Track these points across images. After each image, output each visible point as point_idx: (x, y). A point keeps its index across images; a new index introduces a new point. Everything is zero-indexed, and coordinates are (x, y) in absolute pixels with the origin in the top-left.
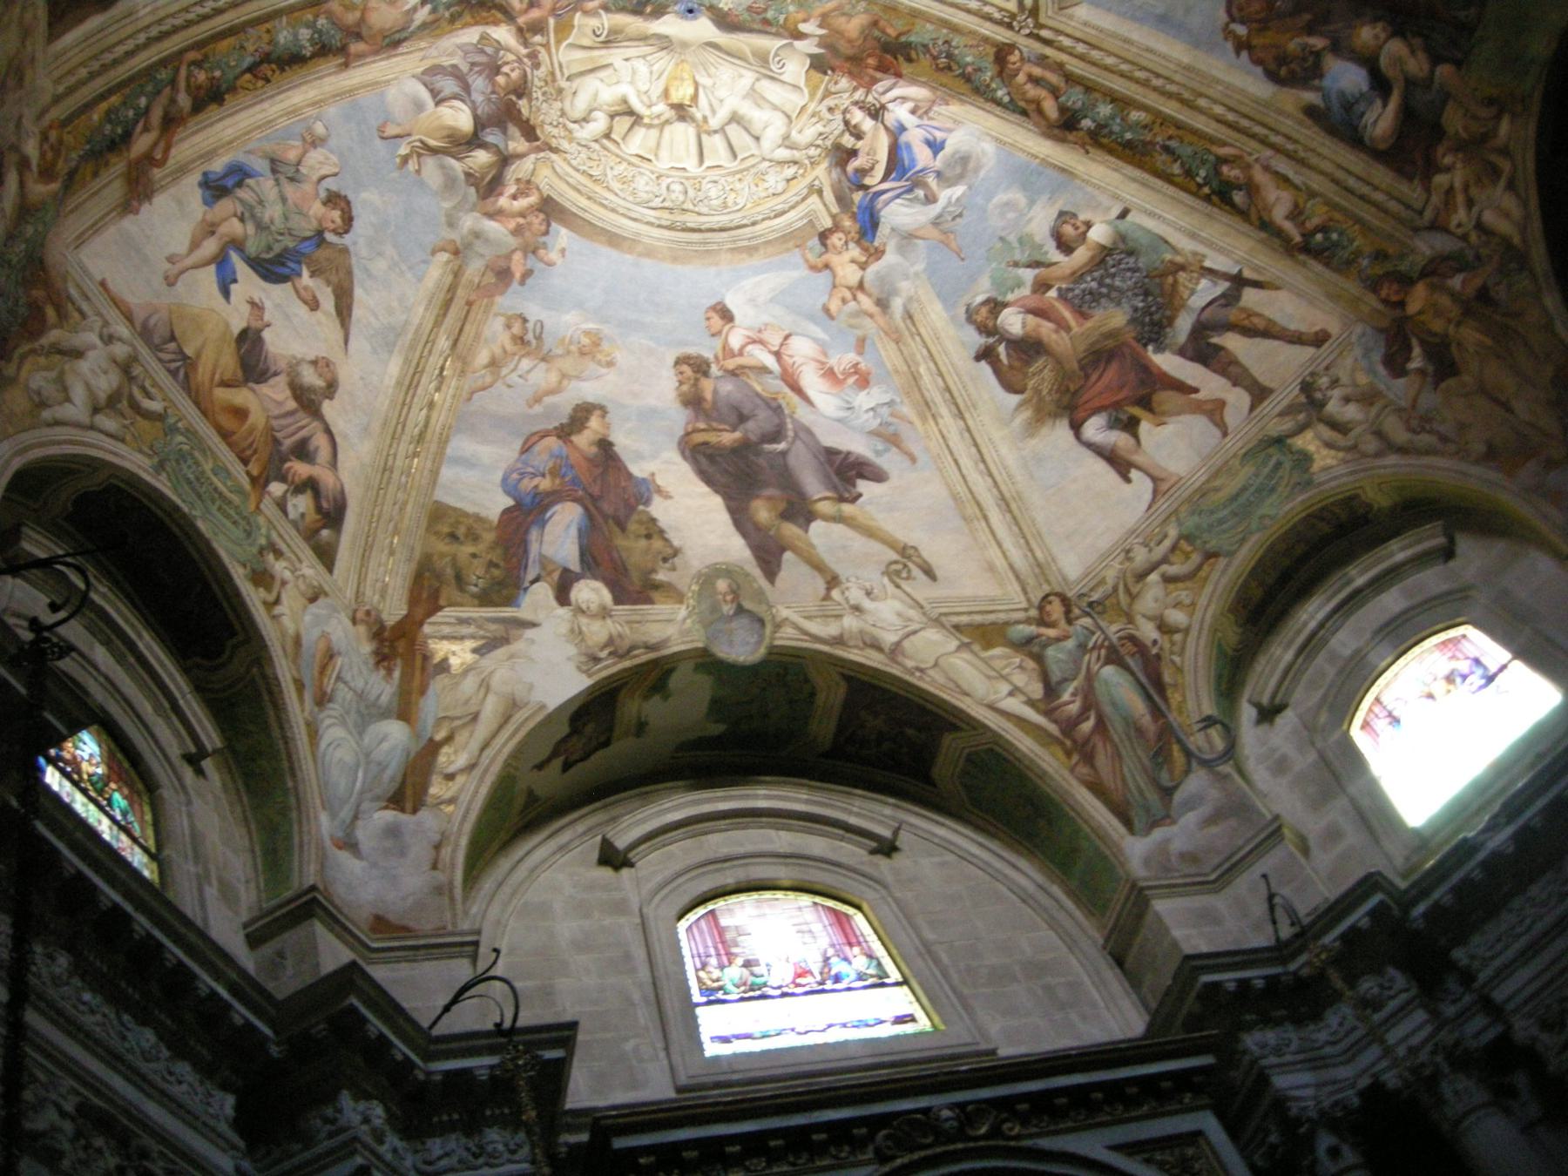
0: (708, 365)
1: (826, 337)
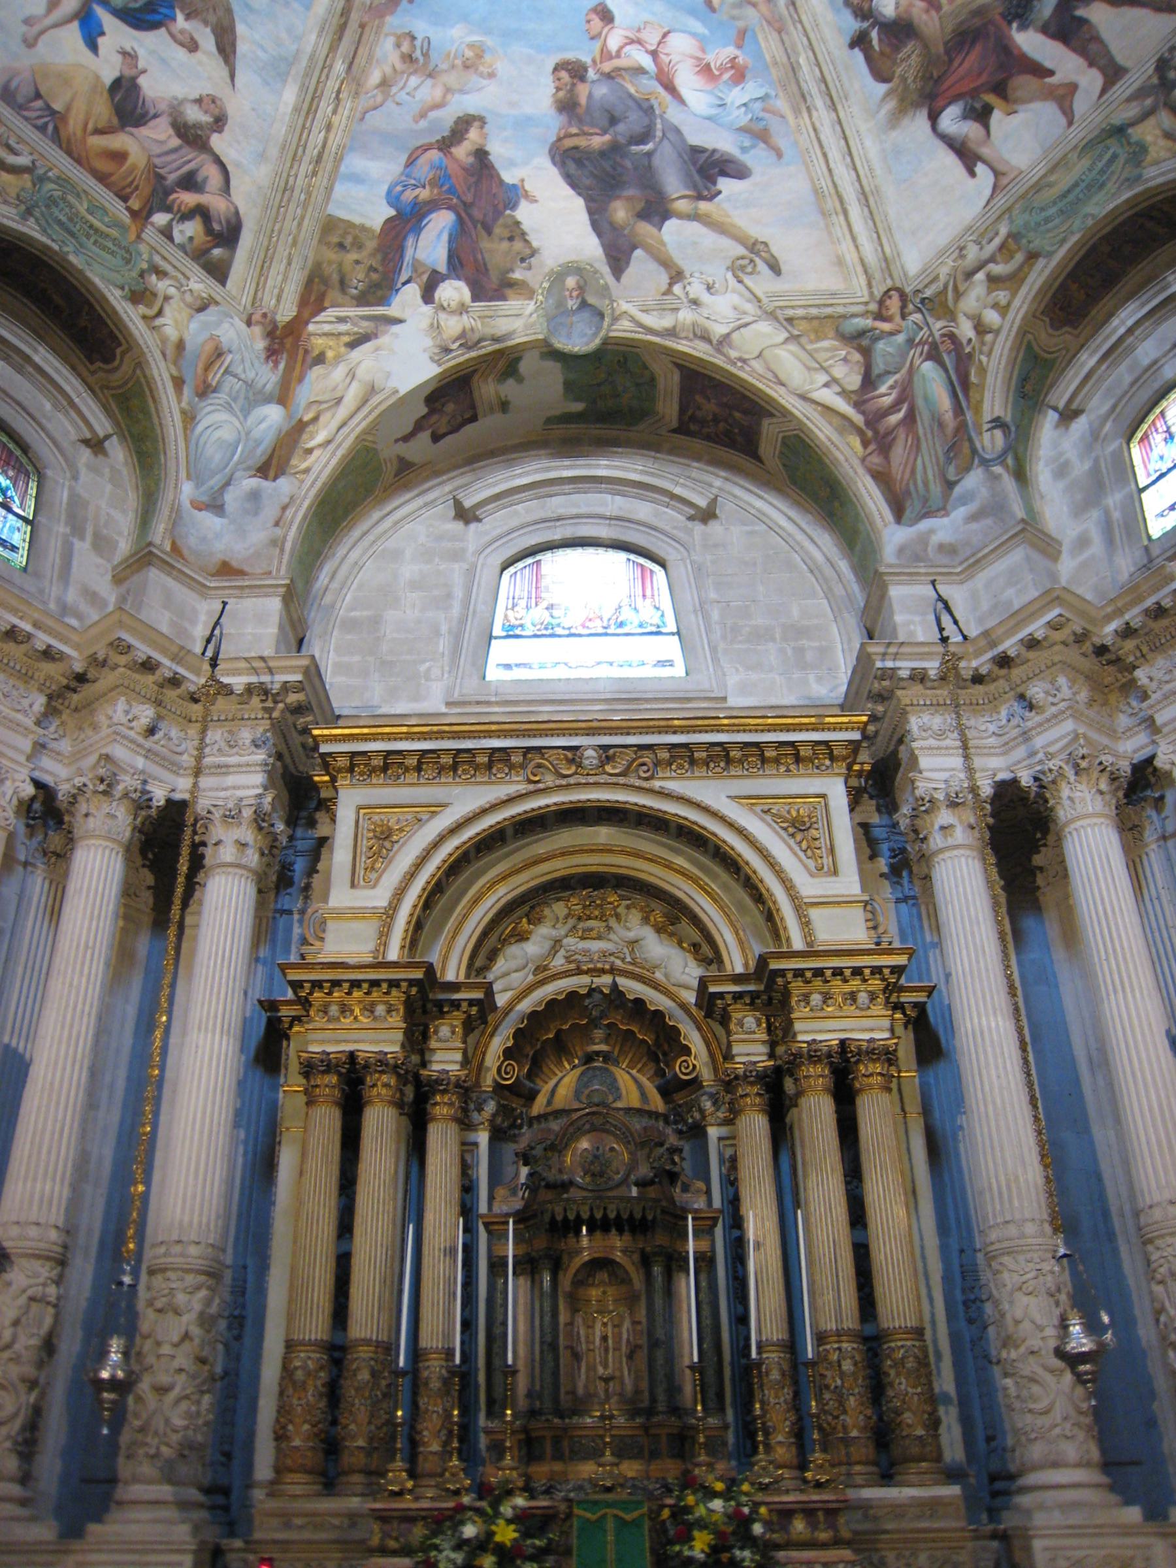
0: (586, 70)
1: (706, 32)
